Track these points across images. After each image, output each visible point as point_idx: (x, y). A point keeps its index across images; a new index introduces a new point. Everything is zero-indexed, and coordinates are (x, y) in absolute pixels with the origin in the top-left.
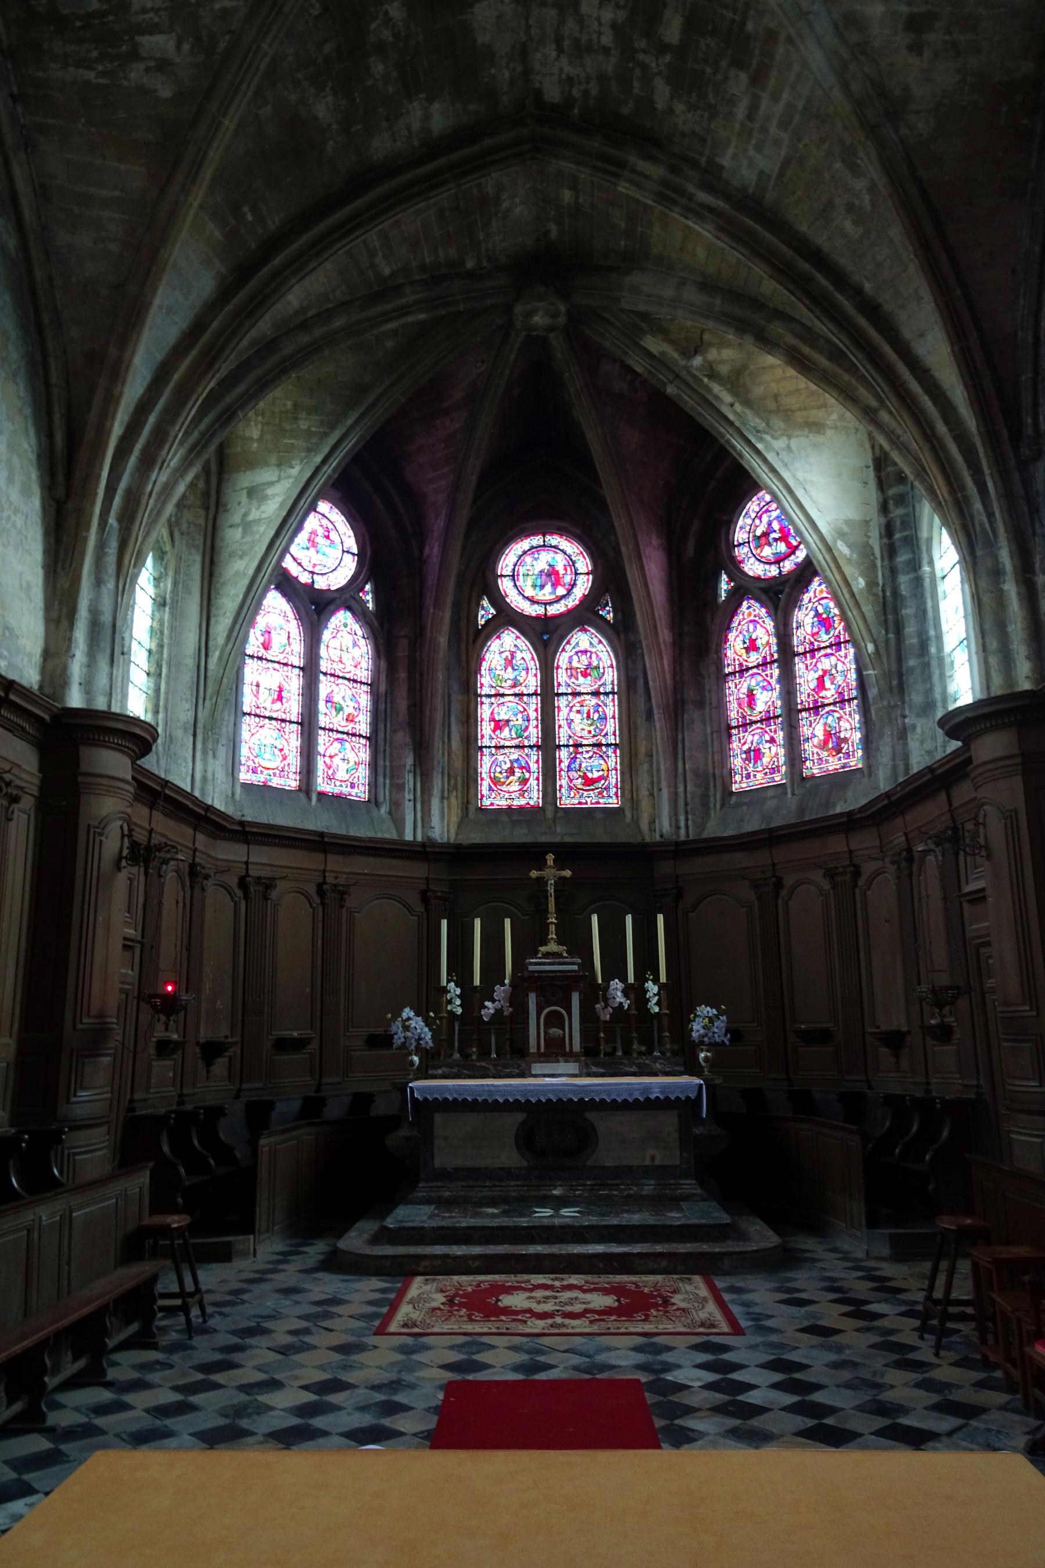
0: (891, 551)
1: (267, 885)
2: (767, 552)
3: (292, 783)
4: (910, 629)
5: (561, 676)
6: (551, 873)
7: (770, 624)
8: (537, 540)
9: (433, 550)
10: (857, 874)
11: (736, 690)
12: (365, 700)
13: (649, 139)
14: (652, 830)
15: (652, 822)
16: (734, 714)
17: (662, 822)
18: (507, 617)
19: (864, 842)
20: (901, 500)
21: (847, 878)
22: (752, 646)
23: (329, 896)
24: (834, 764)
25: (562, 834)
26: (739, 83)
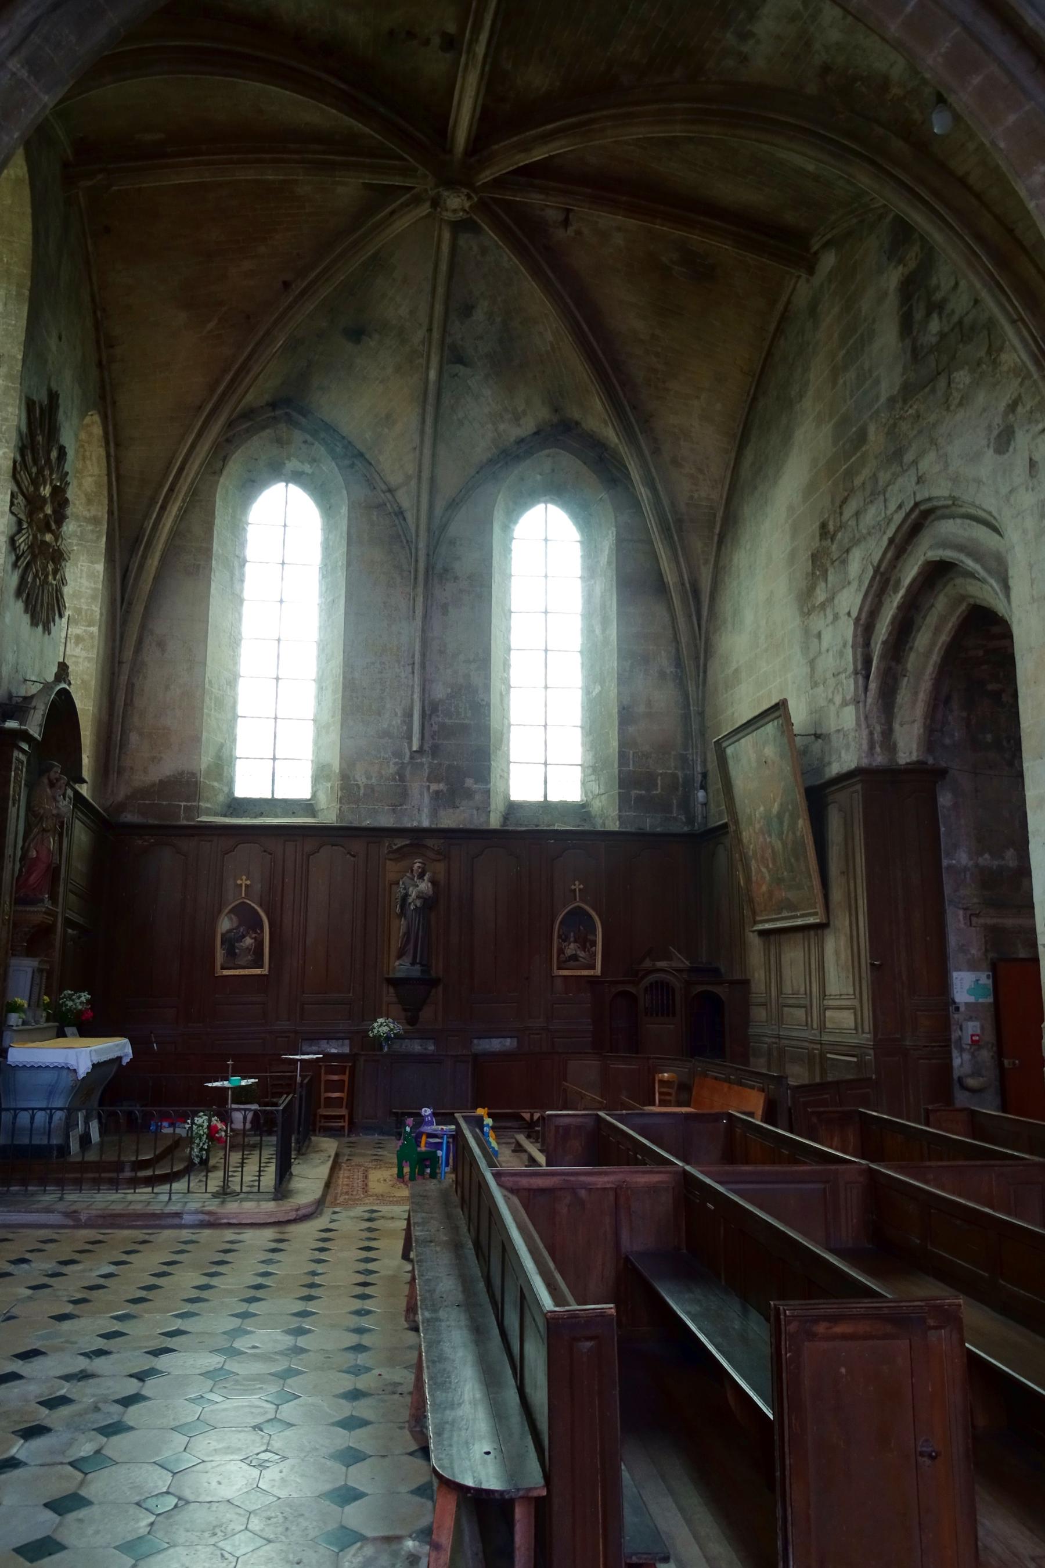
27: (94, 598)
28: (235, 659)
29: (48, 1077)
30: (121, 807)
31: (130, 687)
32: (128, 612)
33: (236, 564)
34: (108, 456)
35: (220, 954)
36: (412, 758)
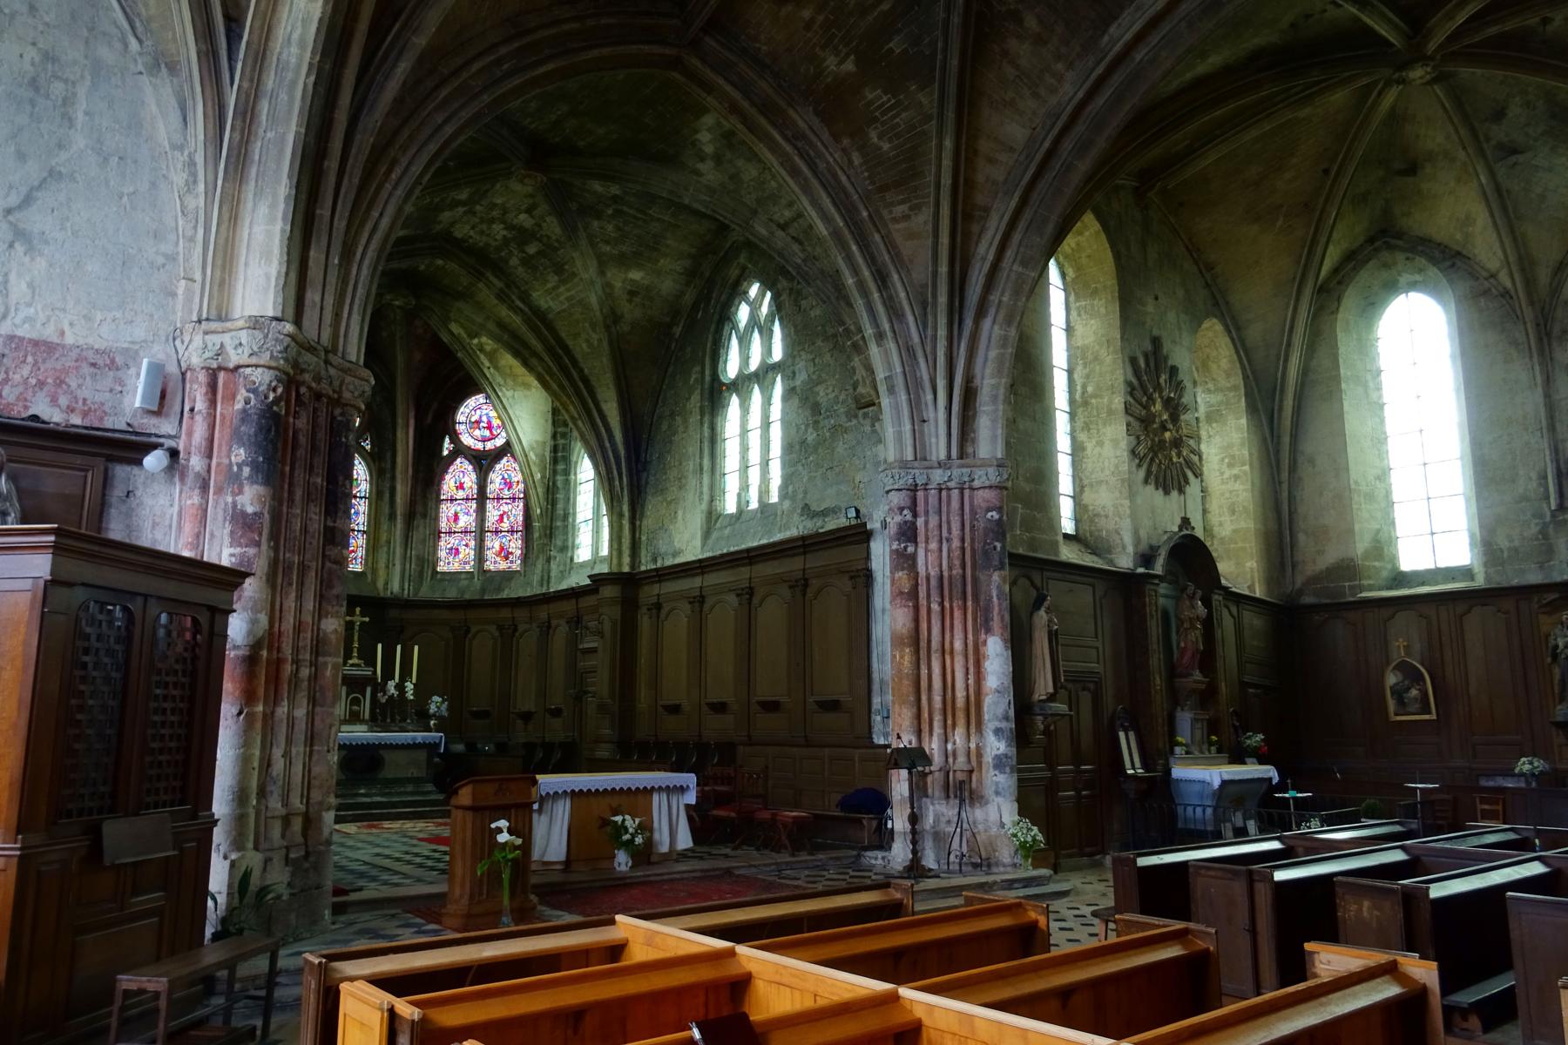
0: (555, 461)
2: (477, 433)
4: (560, 506)
7: (474, 476)
10: (515, 630)
11: (446, 511)
13: (499, 268)
14: (386, 589)
15: (386, 583)
16: (443, 525)
17: (394, 583)
19: (521, 614)
20: (564, 435)
21: (508, 632)
22: (461, 487)
24: (503, 565)
26: (553, 279)
27: (1242, 444)
28: (1382, 454)
29: (1197, 787)
30: (1300, 592)
31: (1291, 499)
32: (1279, 443)
33: (1369, 377)
34: (1232, 340)
35: (1391, 705)
36: (1553, 516)
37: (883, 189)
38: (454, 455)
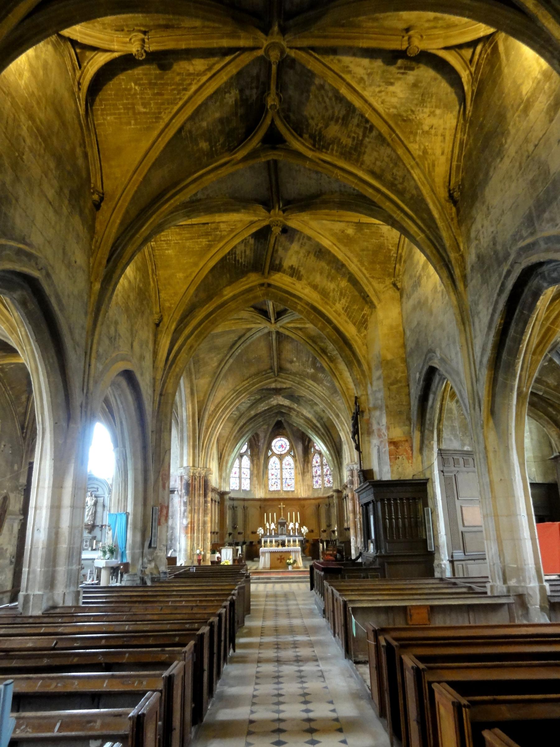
1: (236, 507)
3: (237, 488)
5: (284, 465)
6: (282, 505)
8: (279, 439)
9: (260, 444)
11: (314, 470)
12: (249, 471)
18: (274, 454)
19: (331, 499)
22: (317, 462)
23: (245, 508)
24: (329, 485)
25: (284, 496)
37: (332, 394)
38: (315, 453)
